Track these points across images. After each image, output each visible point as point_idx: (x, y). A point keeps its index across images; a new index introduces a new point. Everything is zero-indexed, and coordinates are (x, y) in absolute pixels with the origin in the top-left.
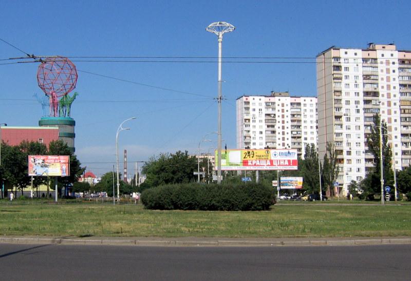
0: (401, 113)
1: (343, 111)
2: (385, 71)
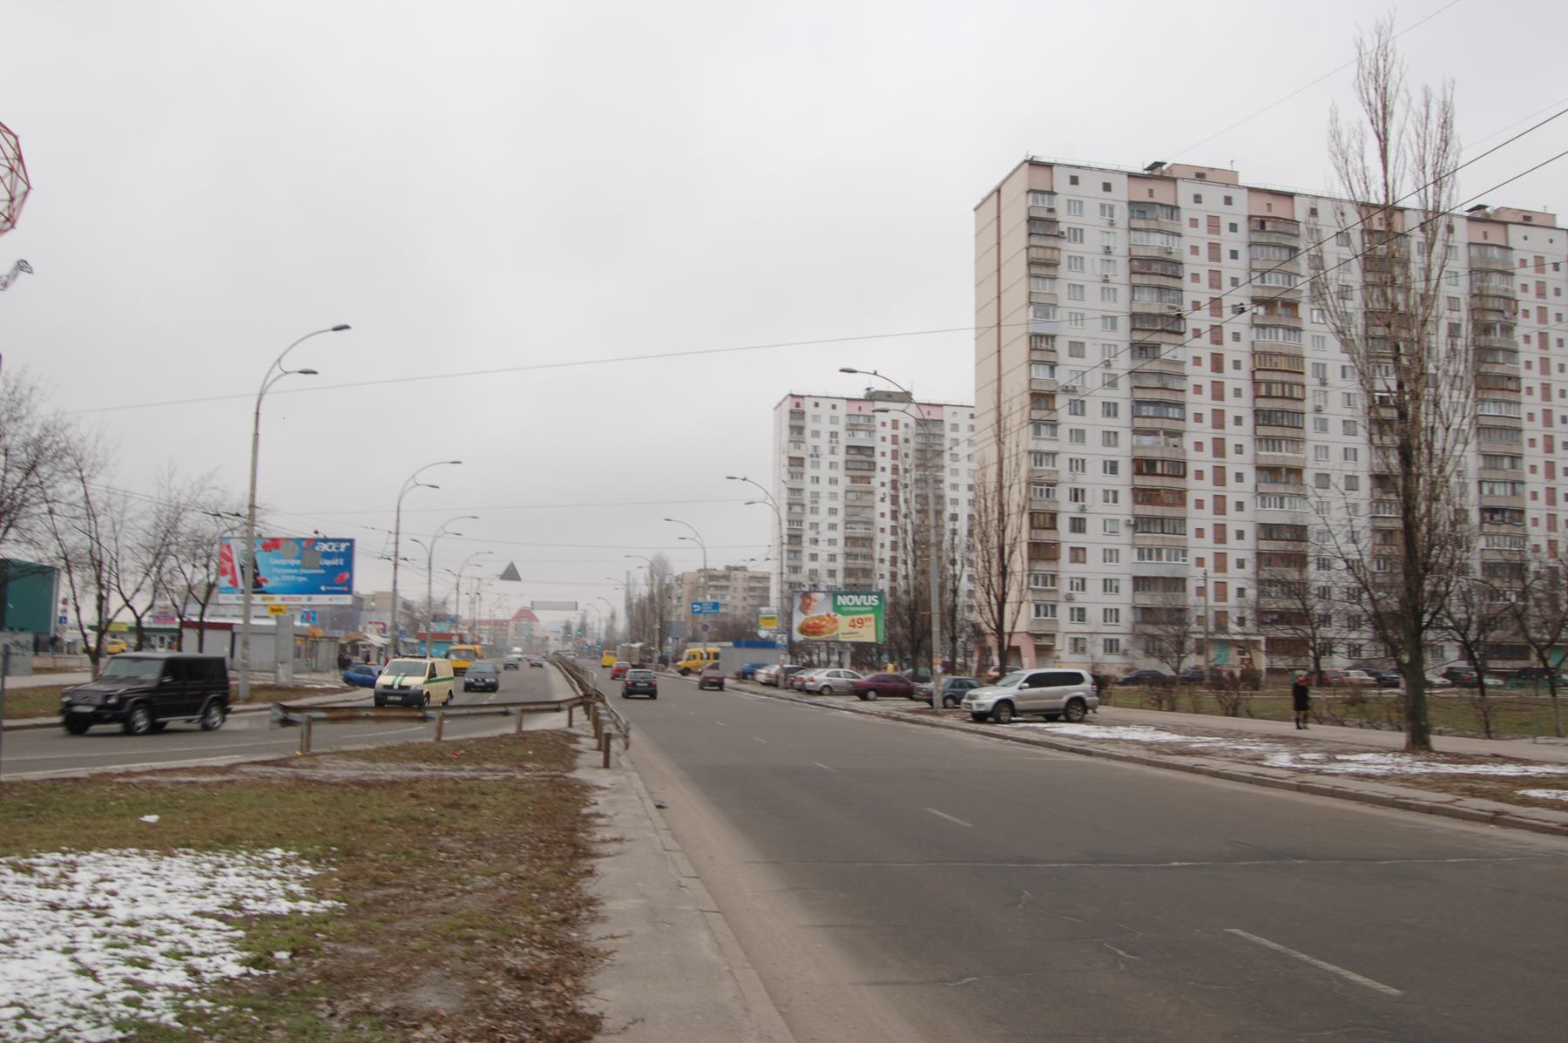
0: (1256, 397)
1: (1063, 377)
2: (1204, 250)
